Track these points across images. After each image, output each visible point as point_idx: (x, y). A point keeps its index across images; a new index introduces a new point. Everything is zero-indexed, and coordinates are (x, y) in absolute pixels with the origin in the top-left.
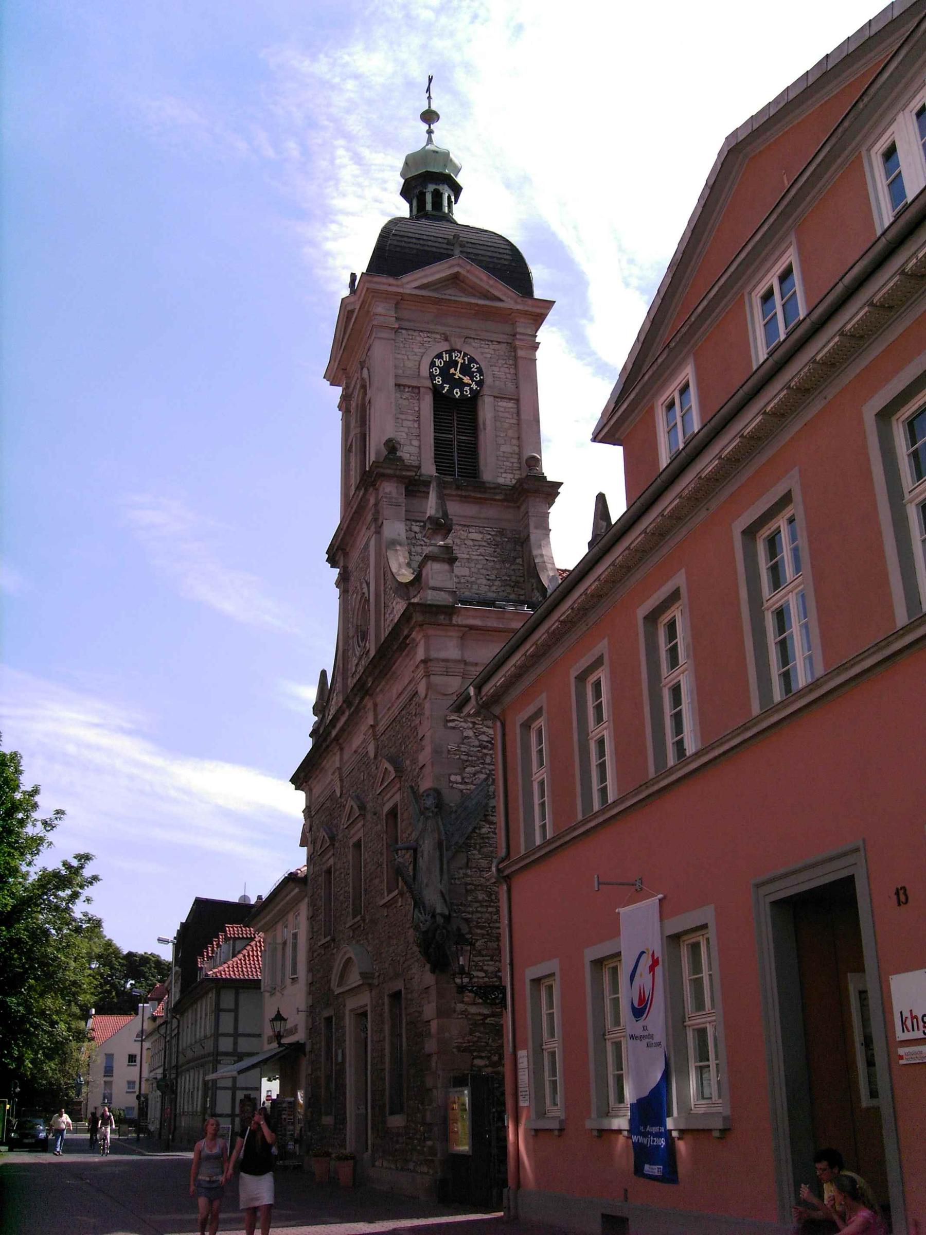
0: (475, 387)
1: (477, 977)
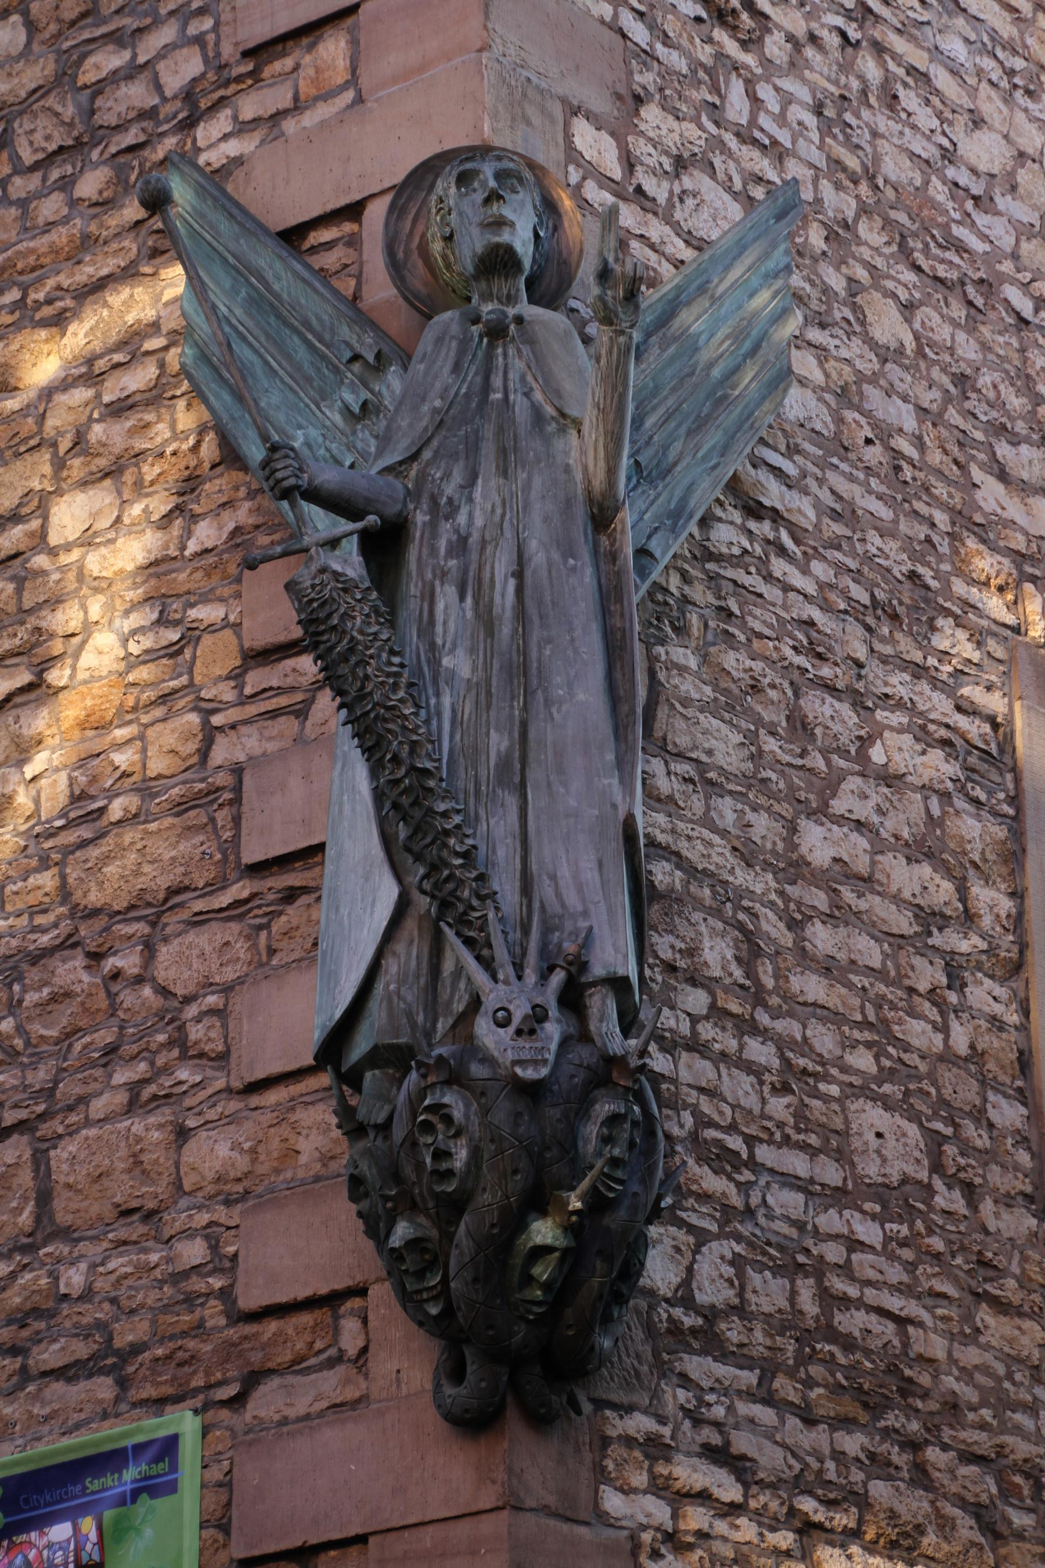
1: (703, 1497)
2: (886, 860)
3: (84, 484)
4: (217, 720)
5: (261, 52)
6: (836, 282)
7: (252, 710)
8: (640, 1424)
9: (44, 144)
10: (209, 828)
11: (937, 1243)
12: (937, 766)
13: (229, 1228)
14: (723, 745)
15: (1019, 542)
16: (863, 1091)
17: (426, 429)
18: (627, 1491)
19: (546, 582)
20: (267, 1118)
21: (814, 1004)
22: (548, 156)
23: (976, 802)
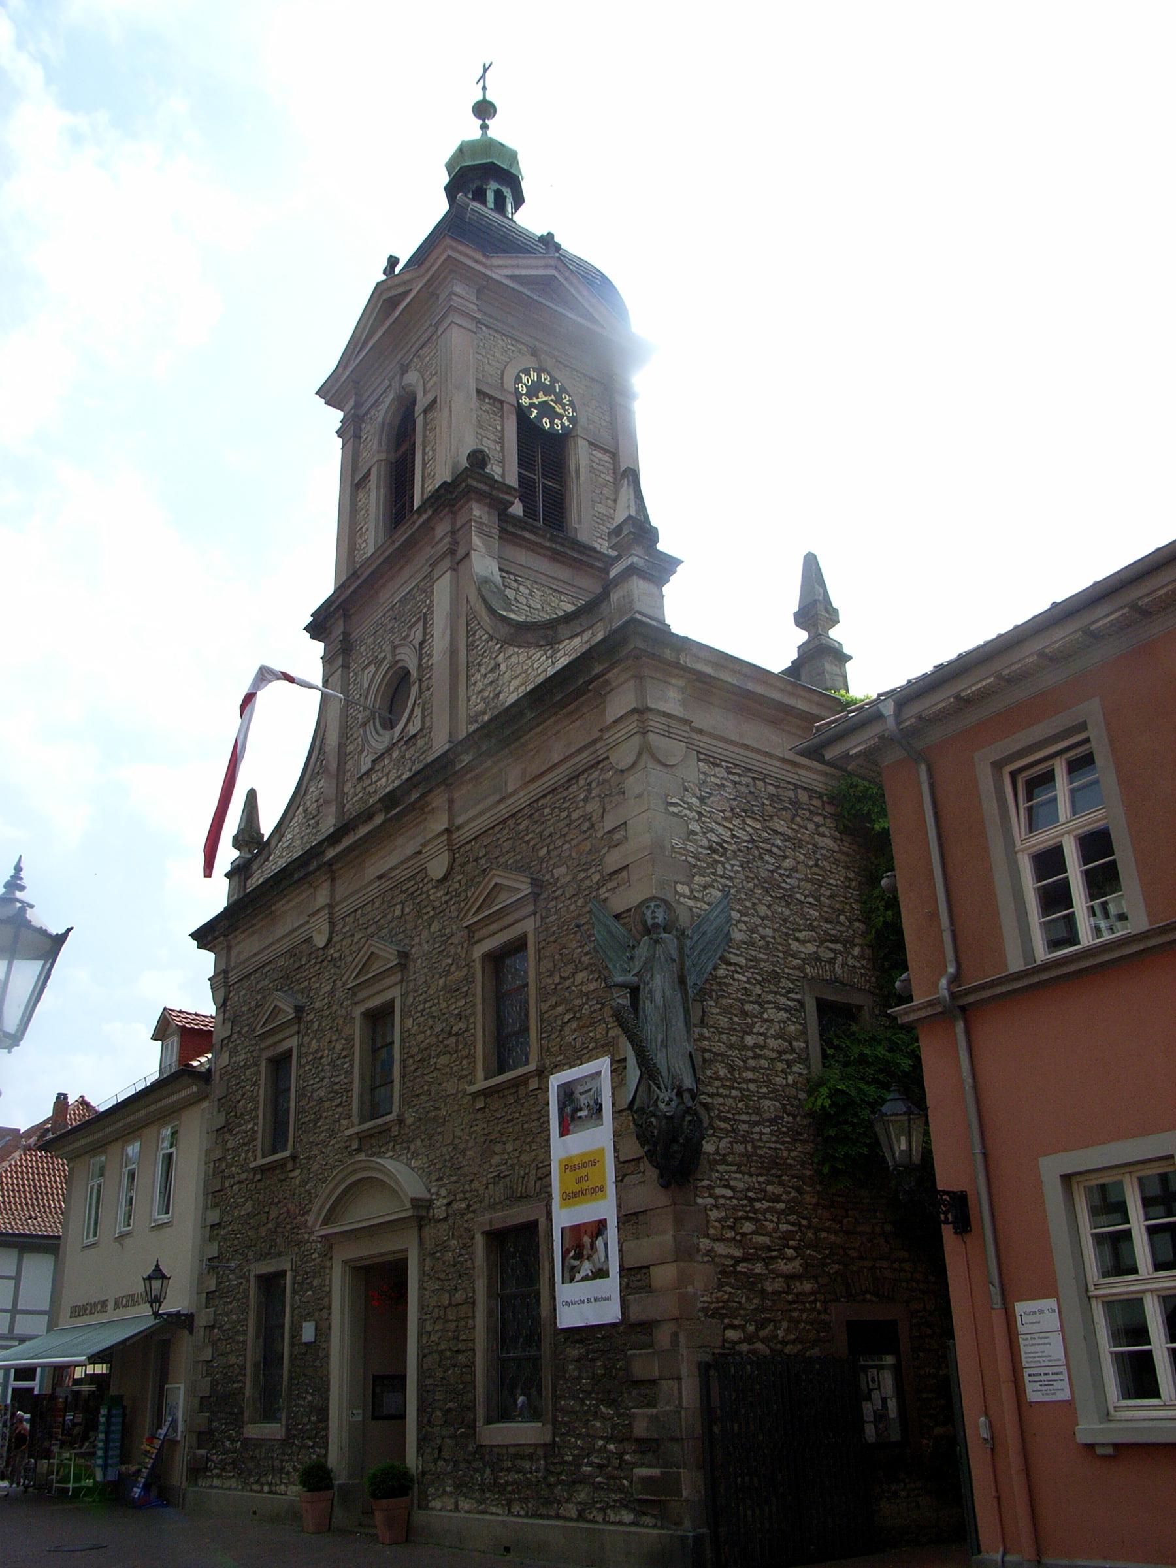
0: (567, 423)
1: (723, 1196)
2: (768, 1041)
5: (611, 874)
6: (748, 904)
8: (706, 1183)
11: (784, 1129)
12: (783, 1015)
14: (723, 1021)
15: (803, 956)
16: (765, 1097)
18: (703, 1197)
22: (669, 897)
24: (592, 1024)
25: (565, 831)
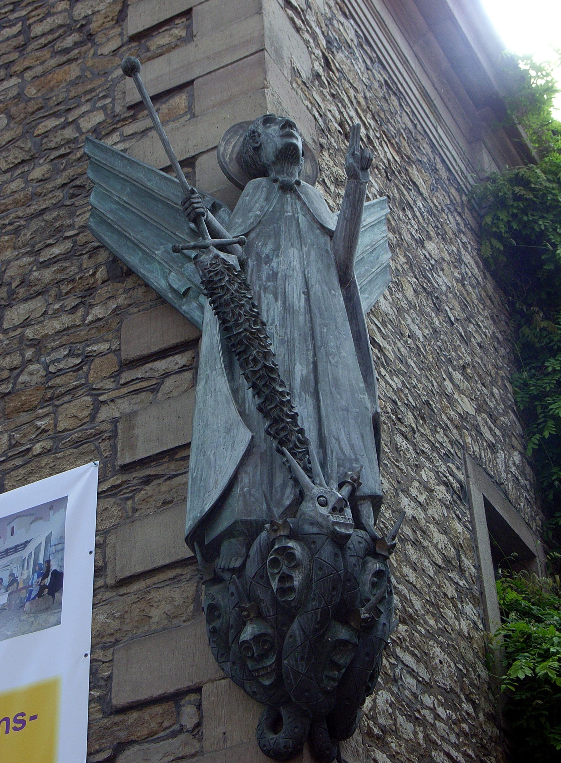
3: (26, 300)
4: (101, 398)
7: (125, 390)
9: (14, 161)
10: (96, 452)
13: (104, 662)
15: (460, 410)
17: (252, 223)
19: (321, 299)
20: (132, 598)
21: (411, 583)
23: (457, 516)
24: (46, 401)
25: (14, 56)
